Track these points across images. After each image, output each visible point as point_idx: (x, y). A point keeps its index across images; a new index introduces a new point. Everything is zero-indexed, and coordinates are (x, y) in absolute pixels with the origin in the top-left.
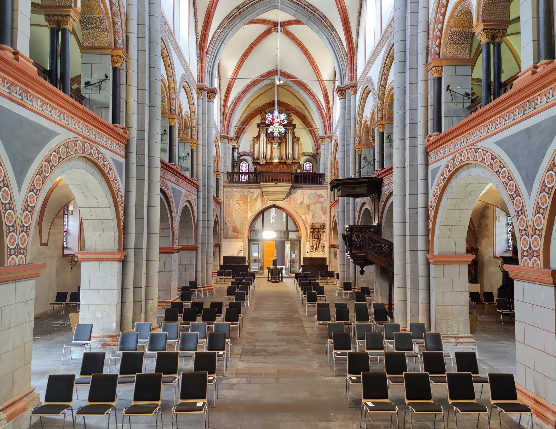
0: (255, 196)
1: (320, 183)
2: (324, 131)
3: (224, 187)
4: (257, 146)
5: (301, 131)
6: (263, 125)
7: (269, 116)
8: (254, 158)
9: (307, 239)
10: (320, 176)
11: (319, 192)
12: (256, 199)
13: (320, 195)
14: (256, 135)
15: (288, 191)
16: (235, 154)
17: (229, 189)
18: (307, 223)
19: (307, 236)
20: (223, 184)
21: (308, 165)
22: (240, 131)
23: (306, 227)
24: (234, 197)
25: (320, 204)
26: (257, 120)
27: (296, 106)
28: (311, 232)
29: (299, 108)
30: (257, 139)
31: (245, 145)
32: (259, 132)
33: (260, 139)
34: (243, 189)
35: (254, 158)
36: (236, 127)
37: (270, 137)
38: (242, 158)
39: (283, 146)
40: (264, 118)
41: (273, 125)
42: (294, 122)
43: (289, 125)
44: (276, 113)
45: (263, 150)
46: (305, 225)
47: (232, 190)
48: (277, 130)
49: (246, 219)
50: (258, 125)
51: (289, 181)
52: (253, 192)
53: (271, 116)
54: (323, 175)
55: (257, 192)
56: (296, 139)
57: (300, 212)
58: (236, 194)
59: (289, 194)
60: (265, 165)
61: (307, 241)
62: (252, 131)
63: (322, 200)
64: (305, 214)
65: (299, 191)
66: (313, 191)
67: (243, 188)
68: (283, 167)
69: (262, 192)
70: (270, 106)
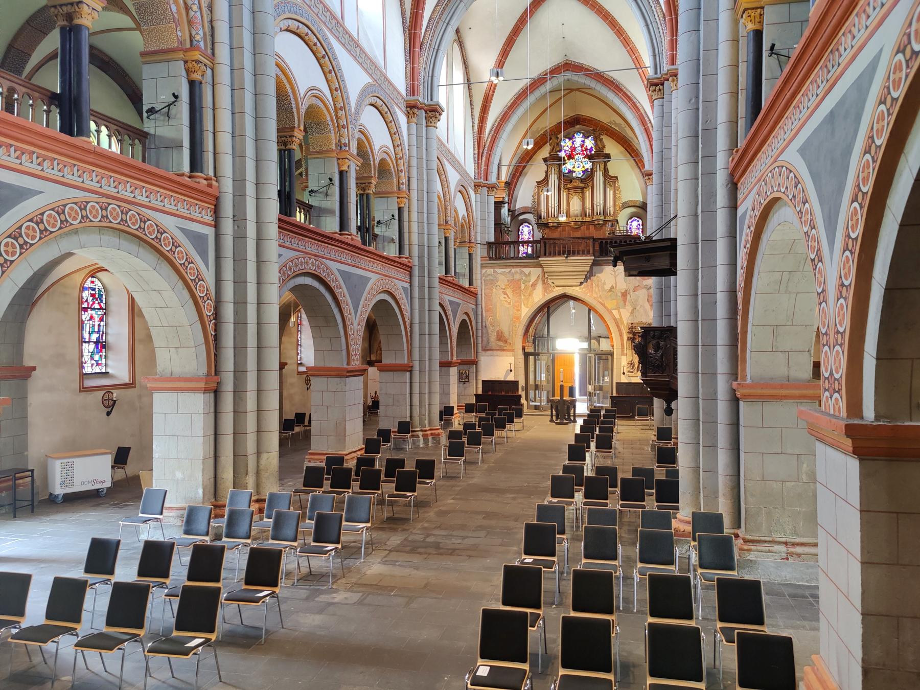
3: (482, 266)
5: (620, 165)
6: (555, 159)
7: (566, 144)
8: (539, 218)
9: (623, 351)
12: (534, 285)
17: (490, 271)
18: (623, 323)
19: (622, 345)
20: (479, 262)
21: (635, 224)
22: (518, 172)
23: (620, 330)
25: (645, 291)
26: (545, 152)
27: (610, 122)
28: (629, 339)
29: (616, 124)
30: (543, 183)
31: (524, 196)
32: (546, 172)
33: (547, 184)
34: (513, 270)
35: (539, 218)
36: (509, 165)
37: (566, 180)
38: (521, 217)
39: (588, 194)
40: (557, 148)
42: (607, 151)
43: (599, 156)
44: (578, 139)
45: (553, 202)
46: (618, 326)
47: (495, 272)
48: (578, 166)
49: (518, 318)
50: (545, 160)
51: (588, 252)
52: (530, 273)
55: (535, 272)
56: (611, 180)
57: (610, 304)
58: (501, 277)
59: (589, 275)
60: (557, 227)
61: (623, 354)
62: (537, 170)
64: (618, 308)
67: (513, 267)
68: (588, 229)
69: (544, 273)
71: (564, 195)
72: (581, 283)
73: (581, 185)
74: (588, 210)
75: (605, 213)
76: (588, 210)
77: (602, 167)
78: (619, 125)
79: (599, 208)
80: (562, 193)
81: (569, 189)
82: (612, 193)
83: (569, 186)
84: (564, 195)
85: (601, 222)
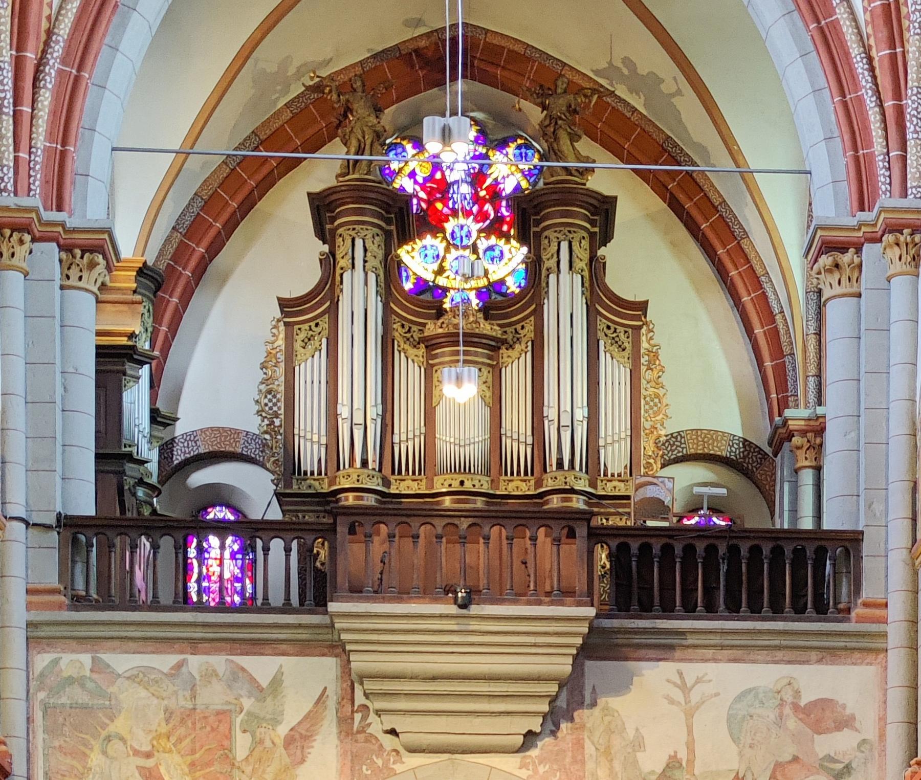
0: (294, 709)
1: (821, 609)
2: (847, 190)
3: (37, 636)
4: (311, 370)
8: (289, 468)
10: (821, 553)
11: (816, 680)
12: (299, 741)
13: (824, 704)
14: (304, 278)
15: (564, 666)
16: (136, 399)
17: (75, 662)
24: (119, 726)
27: (611, 70)
29: (637, 81)
32: (329, 262)
34: (196, 662)
37: (414, 315)
45: (358, 399)
47: (98, 667)
48: (463, 262)
51: (564, 594)
52: (277, 682)
54: (851, 542)
55: (306, 680)
56: (616, 317)
58: (131, 696)
59: (567, 701)
63: (839, 744)
66: (764, 675)
67: (194, 645)
69: (350, 680)
72: (530, 737)
77: (582, 253)
80: (400, 361)
81: (431, 345)
82: (624, 374)
84: (409, 371)
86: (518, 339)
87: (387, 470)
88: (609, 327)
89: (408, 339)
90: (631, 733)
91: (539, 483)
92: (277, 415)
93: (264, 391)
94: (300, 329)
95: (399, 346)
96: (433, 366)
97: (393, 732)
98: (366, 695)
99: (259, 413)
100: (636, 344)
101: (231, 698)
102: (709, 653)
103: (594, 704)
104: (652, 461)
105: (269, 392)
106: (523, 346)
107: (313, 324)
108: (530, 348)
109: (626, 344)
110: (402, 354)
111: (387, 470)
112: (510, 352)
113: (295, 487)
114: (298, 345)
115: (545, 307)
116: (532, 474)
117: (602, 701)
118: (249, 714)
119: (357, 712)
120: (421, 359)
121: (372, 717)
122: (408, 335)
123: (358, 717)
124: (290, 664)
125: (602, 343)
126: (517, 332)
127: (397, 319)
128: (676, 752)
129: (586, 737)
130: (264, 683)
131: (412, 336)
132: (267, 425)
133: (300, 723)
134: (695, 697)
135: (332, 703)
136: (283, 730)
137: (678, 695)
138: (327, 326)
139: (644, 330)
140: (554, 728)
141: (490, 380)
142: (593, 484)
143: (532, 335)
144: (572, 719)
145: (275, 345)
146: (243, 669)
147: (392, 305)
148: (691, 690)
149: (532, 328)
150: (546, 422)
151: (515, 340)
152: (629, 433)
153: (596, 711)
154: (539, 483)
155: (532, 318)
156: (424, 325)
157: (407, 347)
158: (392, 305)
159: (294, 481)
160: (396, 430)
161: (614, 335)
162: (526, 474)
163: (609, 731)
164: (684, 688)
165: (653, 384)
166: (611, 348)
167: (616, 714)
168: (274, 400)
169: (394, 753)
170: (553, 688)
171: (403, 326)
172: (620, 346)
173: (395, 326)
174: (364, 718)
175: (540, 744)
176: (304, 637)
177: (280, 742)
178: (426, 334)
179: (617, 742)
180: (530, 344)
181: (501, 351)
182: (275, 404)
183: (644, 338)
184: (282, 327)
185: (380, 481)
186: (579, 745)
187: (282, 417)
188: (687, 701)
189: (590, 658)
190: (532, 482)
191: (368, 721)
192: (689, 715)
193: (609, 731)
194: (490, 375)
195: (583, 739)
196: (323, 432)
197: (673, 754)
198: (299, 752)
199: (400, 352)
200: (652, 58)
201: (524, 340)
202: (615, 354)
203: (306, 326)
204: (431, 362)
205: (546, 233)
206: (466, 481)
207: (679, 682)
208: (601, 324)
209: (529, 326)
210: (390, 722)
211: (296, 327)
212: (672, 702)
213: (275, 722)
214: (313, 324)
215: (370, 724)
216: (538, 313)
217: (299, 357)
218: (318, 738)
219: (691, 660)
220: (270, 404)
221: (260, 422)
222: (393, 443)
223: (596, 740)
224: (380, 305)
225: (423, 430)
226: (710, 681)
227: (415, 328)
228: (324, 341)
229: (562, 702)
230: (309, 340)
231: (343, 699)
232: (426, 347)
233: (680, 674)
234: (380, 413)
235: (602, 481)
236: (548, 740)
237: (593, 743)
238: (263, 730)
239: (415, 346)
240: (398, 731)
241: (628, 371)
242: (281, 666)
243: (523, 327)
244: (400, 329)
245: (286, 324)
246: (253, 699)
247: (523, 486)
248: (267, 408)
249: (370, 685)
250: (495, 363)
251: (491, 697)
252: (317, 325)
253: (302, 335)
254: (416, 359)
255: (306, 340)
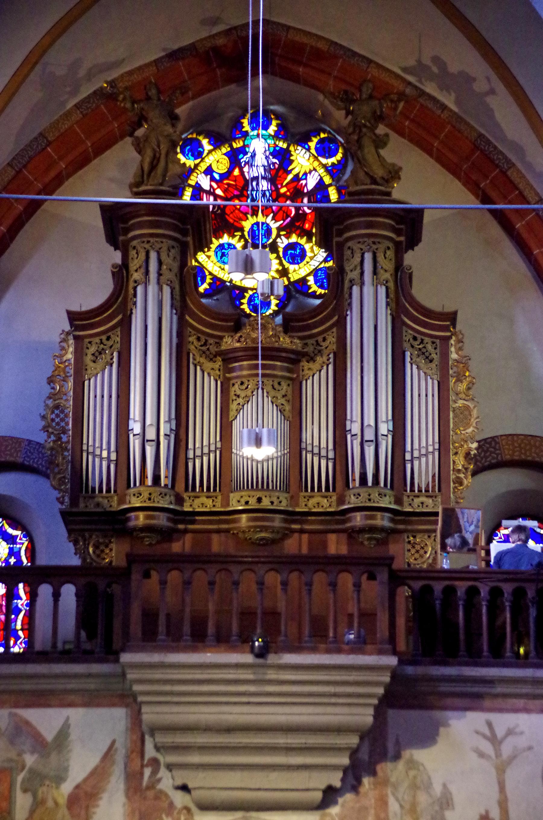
0: (80, 764)
4: (101, 386)
8: (77, 483)
14: (94, 292)
15: (366, 717)
26: (109, 181)
29: (445, 79)
30: (102, 328)
32: (121, 274)
33: (126, 325)
37: (210, 323)
39: (317, 387)
41: (233, 229)
42: (406, 193)
50: (116, 222)
52: (63, 735)
53: (217, 160)
56: (422, 330)
59: (370, 755)
65: (464, 727)
69: (139, 731)
70: (203, 82)
71: (205, 388)
72: (330, 795)
73: (285, 341)
74: (319, 465)
75: (398, 474)
76: (319, 465)
77: (387, 264)
78: (461, 83)
79: (370, 456)
81: (228, 358)
82: (432, 386)
83: (230, 342)
84: (205, 388)
85: (382, 521)
86: (320, 351)
87: (180, 486)
88: (415, 339)
89: (204, 352)
90: (438, 789)
91: (341, 500)
92: (64, 432)
93: (51, 405)
94: (90, 343)
95: (194, 359)
96: (229, 379)
97: (184, 788)
98: (157, 748)
99: (45, 429)
100: (445, 355)
101: (13, 754)
102: (521, 703)
103: (397, 757)
104: (462, 476)
105: (57, 407)
106: (325, 358)
107: (104, 338)
108: (331, 360)
109: (434, 356)
110: (198, 368)
111: (180, 486)
112: (311, 365)
113: (82, 505)
114: (88, 359)
115: (348, 318)
116: (334, 490)
117: (406, 754)
118: (32, 771)
119: (147, 766)
120: (217, 372)
121: (163, 773)
122: (204, 348)
123: (147, 772)
124: (76, 715)
125: (408, 354)
126: (318, 344)
127: (193, 332)
128: (487, 812)
129: (389, 792)
130: (49, 736)
131: (208, 349)
132: (54, 441)
133: (86, 780)
134: (506, 749)
135: (120, 757)
136: (67, 788)
137: (487, 747)
138: (118, 339)
139: (452, 341)
140: (355, 783)
141: (290, 393)
142: (398, 501)
143: (334, 347)
144: (374, 773)
145: (65, 358)
146: (27, 723)
147: (187, 318)
148: (501, 742)
149: (334, 340)
150: (349, 437)
151: (316, 352)
152: (437, 446)
153: (401, 765)
154: (341, 500)
155: (334, 330)
156: (221, 338)
157: (202, 360)
158: (187, 318)
159: (81, 500)
160: (191, 446)
161: (420, 346)
162: (327, 489)
163: (414, 787)
164: (494, 740)
165: (463, 396)
166: (418, 360)
167: (421, 768)
168: (62, 416)
169: (185, 811)
170: (354, 740)
171: (199, 339)
172: (427, 358)
173: (191, 339)
174: (155, 772)
175: (340, 800)
176: (92, 687)
177: (62, 801)
178: (223, 348)
179: (423, 798)
180: (331, 356)
181: (302, 364)
182: (62, 420)
183: (453, 349)
184: (71, 341)
185: (173, 498)
186: (383, 802)
187: (70, 432)
188: (498, 754)
189: (392, 706)
190: (334, 498)
191: (159, 776)
192: (501, 770)
193: (414, 787)
194: (290, 389)
195: (387, 795)
196: (113, 448)
197: (483, 812)
198: (83, 813)
199: (195, 366)
200: (462, 58)
201: (326, 352)
202: (422, 365)
203: (97, 340)
204: (227, 375)
205: (350, 244)
206: (264, 498)
207: (487, 732)
208: (407, 335)
209: (332, 339)
210: (181, 777)
211: (87, 340)
212: (481, 755)
213: (60, 779)
214: (104, 338)
215: (159, 780)
216: (341, 325)
217: (89, 372)
218: (105, 796)
219: (501, 710)
220: (57, 420)
221: (46, 438)
222: (187, 459)
223: (400, 796)
224: (175, 318)
225: (219, 445)
226: (522, 733)
227: (211, 341)
228: (115, 354)
229: (364, 755)
230: (100, 353)
231: (132, 752)
232: (223, 360)
233: (490, 724)
234: (174, 428)
235: (408, 496)
236: (349, 797)
237: (397, 800)
238: (45, 789)
239: (211, 359)
240: (190, 786)
241: (436, 382)
242: (68, 718)
243: (324, 340)
244: (196, 342)
245: (76, 338)
246: (36, 756)
247: (325, 502)
248: (54, 424)
249: (161, 739)
250: (295, 376)
251: (289, 750)
252: (108, 338)
253: (93, 349)
254: (212, 372)
255: (97, 354)
